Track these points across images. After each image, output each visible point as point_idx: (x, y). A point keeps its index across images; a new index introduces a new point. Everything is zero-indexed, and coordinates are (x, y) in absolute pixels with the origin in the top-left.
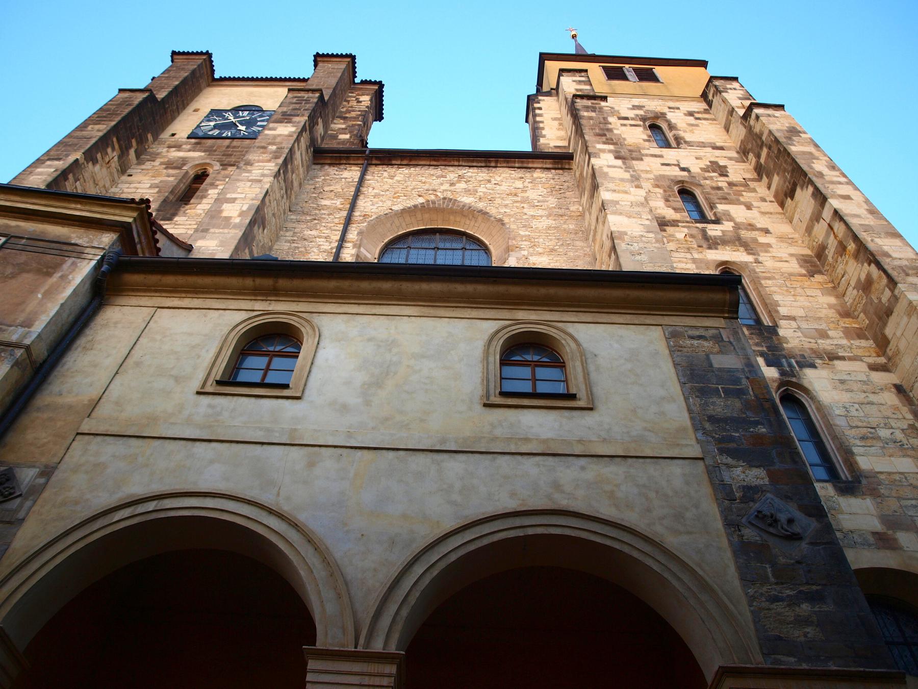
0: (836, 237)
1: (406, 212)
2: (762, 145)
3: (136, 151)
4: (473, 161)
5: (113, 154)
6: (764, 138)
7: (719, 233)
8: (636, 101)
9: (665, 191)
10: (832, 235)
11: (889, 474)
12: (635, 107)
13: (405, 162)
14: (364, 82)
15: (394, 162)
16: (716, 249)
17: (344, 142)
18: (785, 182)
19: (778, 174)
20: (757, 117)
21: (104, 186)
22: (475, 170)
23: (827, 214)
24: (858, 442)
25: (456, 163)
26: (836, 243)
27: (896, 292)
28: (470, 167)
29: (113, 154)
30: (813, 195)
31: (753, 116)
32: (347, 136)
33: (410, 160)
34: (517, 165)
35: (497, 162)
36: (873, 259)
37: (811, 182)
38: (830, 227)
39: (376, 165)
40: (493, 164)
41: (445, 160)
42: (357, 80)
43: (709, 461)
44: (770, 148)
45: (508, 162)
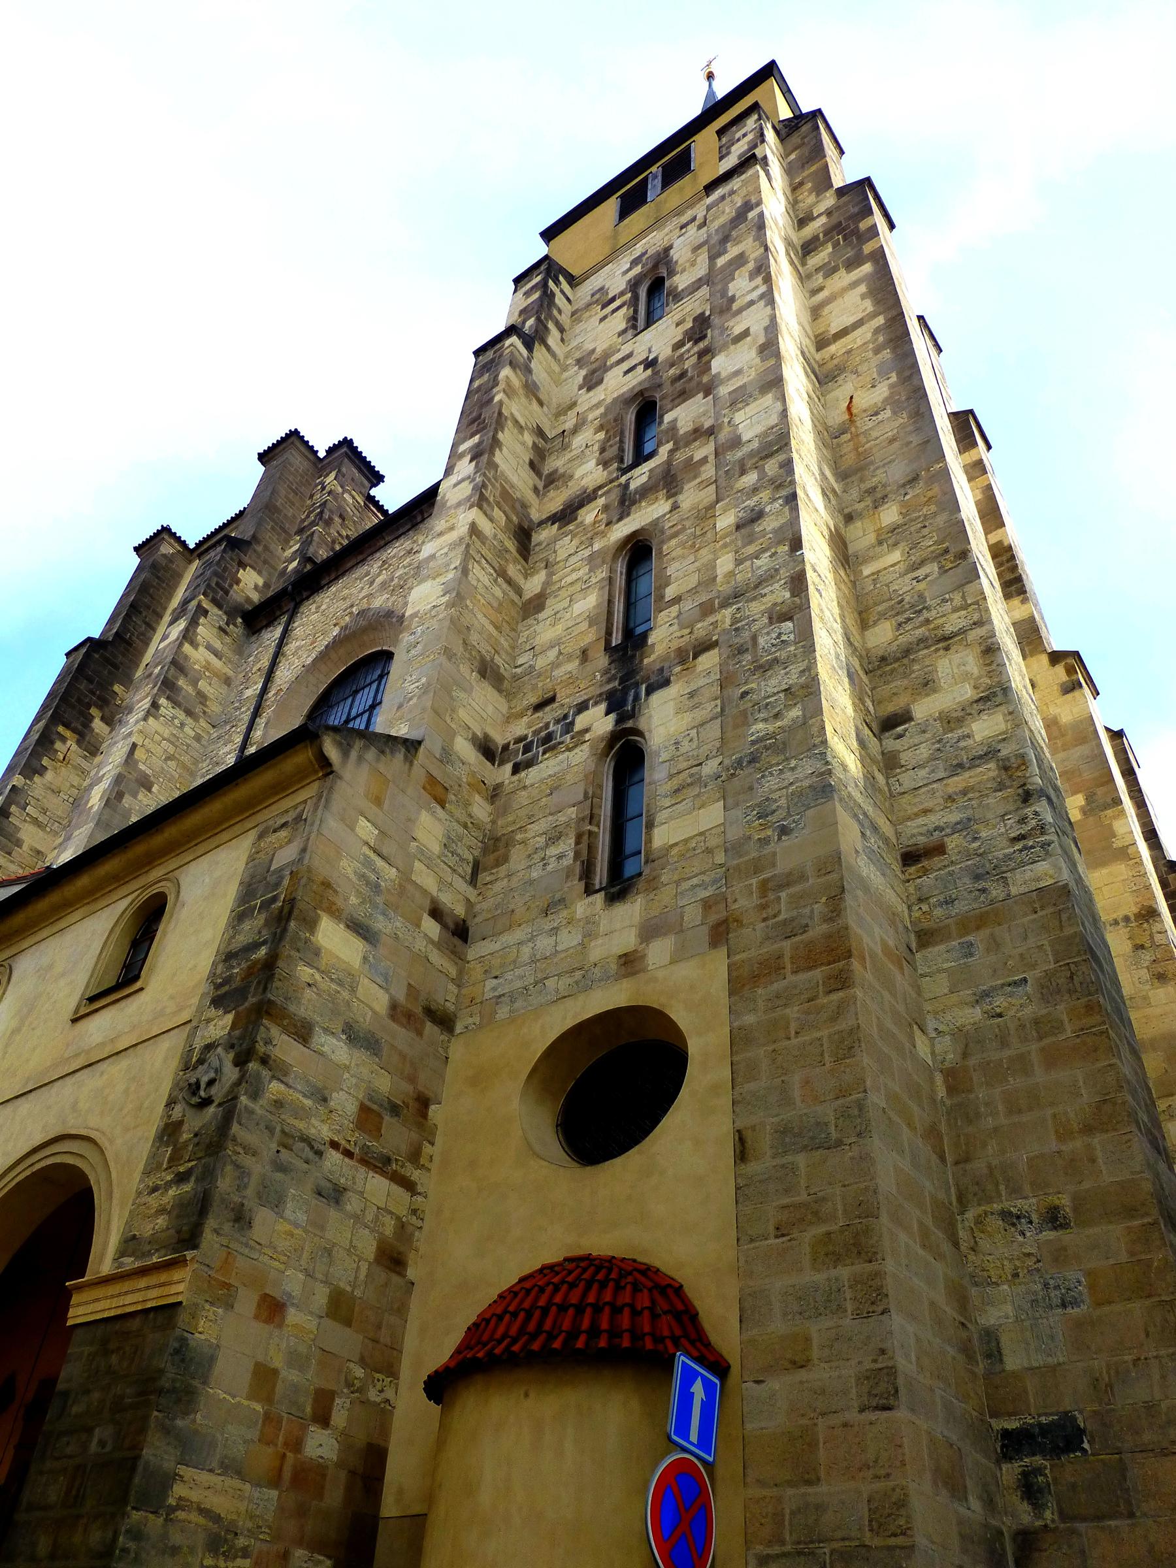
1: (323, 656)
3: (102, 719)
4: (398, 529)
5: (68, 745)
7: (644, 478)
8: (638, 250)
9: (607, 432)
11: (686, 841)
12: (635, 262)
13: (333, 576)
14: (330, 451)
15: (323, 582)
16: (628, 515)
17: (296, 570)
21: (73, 786)
22: (402, 540)
24: (667, 802)
25: (382, 543)
28: (397, 538)
29: (68, 745)
32: (295, 564)
33: (337, 570)
35: (422, 513)
39: (307, 598)
40: (419, 518)
41: (370, 547)
42: (322, 454)
43: (194, 1024)
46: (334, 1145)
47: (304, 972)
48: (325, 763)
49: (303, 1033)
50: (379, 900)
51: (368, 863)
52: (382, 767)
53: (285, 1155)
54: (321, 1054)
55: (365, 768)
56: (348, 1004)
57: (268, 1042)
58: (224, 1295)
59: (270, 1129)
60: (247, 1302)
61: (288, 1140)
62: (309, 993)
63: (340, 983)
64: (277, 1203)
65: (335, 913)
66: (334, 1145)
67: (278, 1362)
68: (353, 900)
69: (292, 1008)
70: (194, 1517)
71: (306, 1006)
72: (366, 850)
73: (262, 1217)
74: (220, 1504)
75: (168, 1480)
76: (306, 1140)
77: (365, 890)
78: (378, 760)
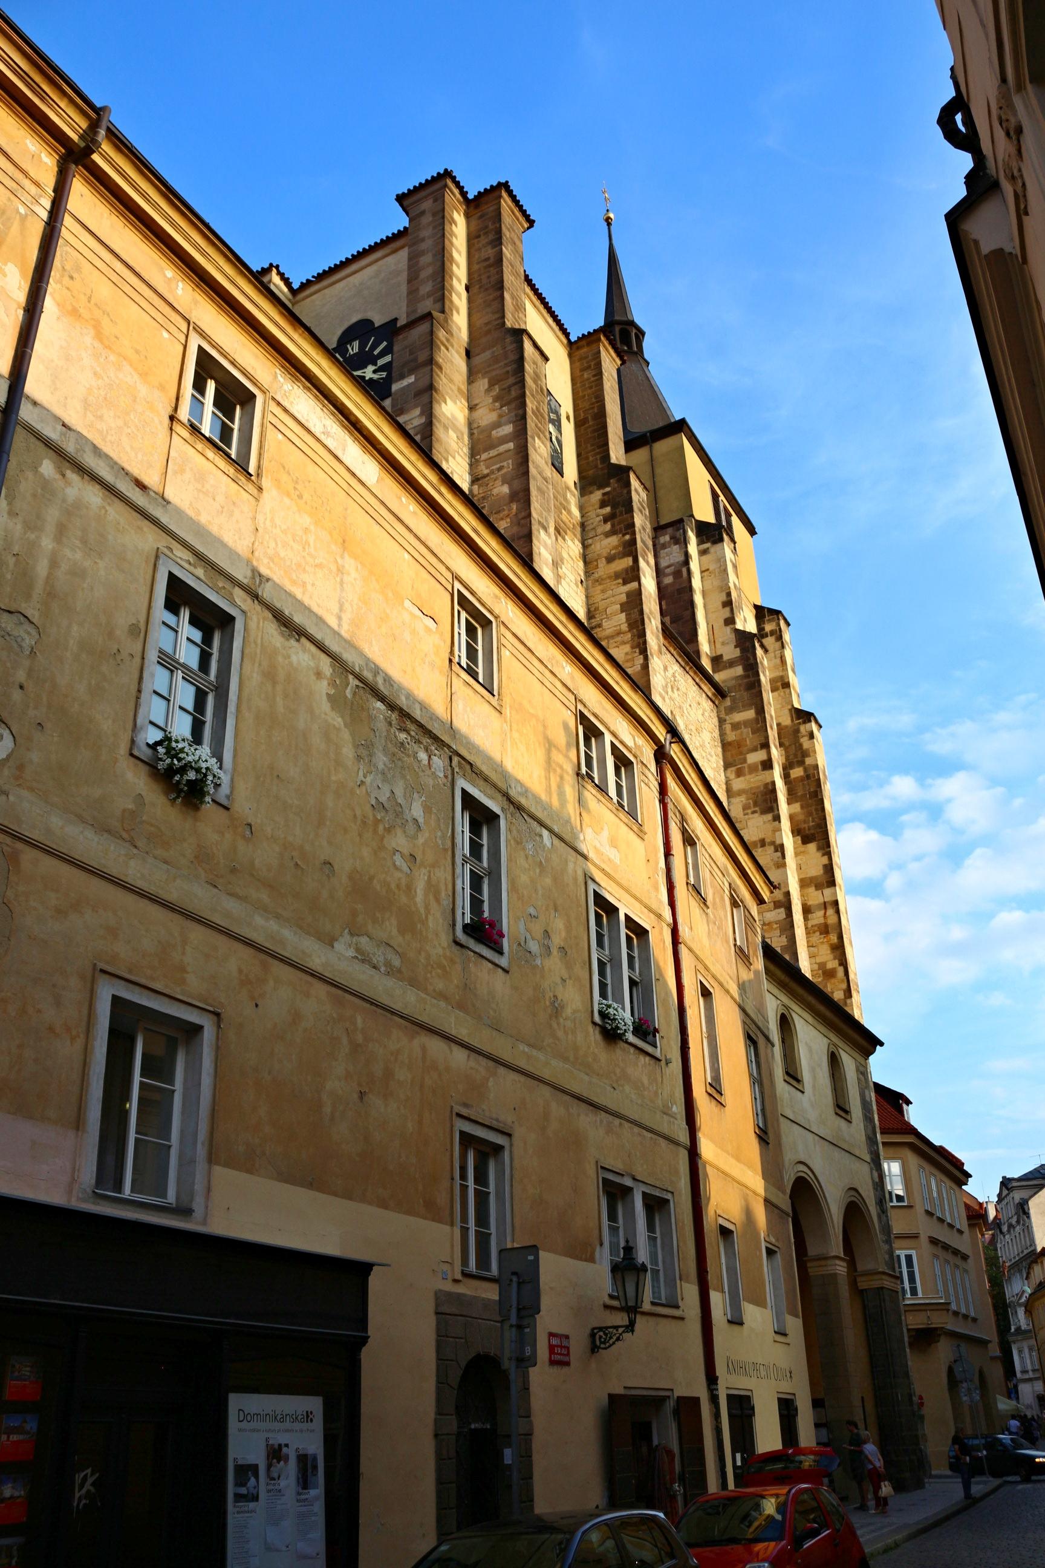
0: (825, 916)
2: (801, 763)
4: (681, 656)
6: (808, 761)
10: (822, 912)
18: (805, 822)
19: (802, 807)
20: (811, 736)
23: (827, 892)
26: (822, 921)
27: (848, 1001)
30: (825, 866)
31: (808, 725)
34: (697, 680)
36: (844, 963)
37: (829, 854)
38: (825, 905)
44: (808, 777)
45: (695, 673)
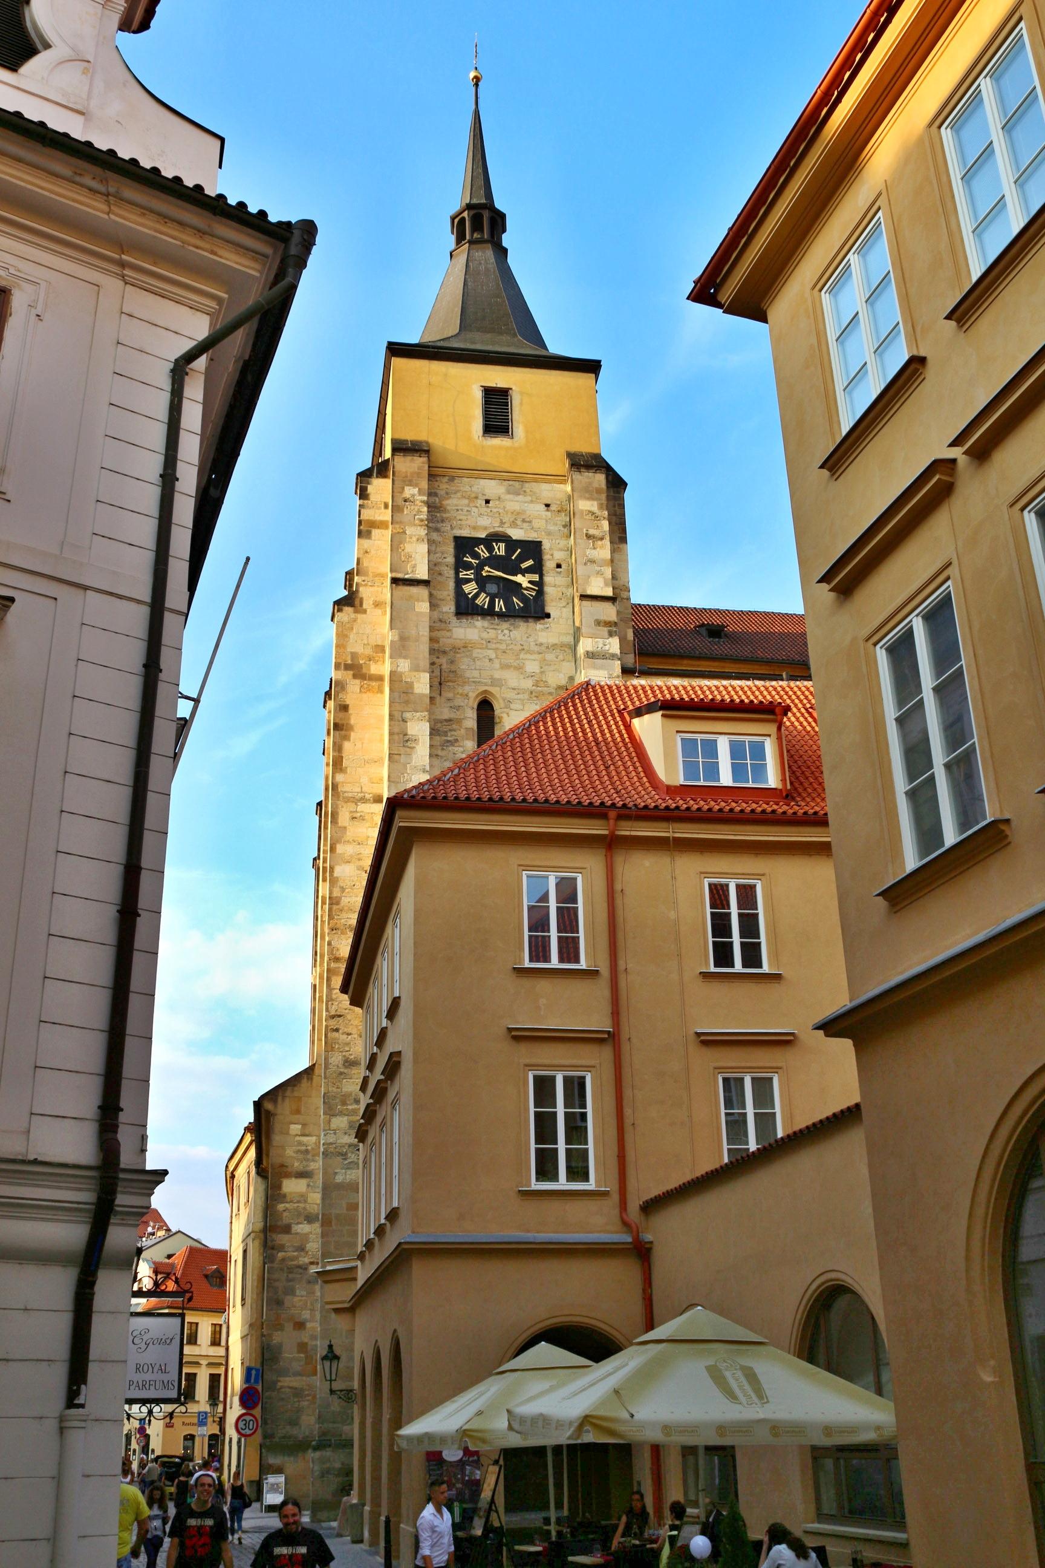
46: (312, 1263)
47: (281, 1207)
48: (268, 1112)
49: (287, 1229)
50: (309, 1157)
51: (300, 1143)
52: (296, 1094)
53: (291, 1276)
54: (297, 1234)
55: (287, 1101)
56: (304, 1208)
57: (273, 1240)
58: (279, 1327)
59: (282, 1269)
60: (289, 1327)
61: (290, 1270)
62: (285, 1214)
63: (298, 1202)
64: (291, 1292)
65: (288, 1175)
66: (312, 1263)
67: (306, 1340)
68: (296, 1164)
69: (279, 1223)
70: (288, 1390)
71: (286, 1218)
72: (298, 1138)
73: (288, 1300)
74: (294, 1384)
75: (275, 1383)
76: (299, 1267)
77: (301, 1156)
78: (293, 1091)
